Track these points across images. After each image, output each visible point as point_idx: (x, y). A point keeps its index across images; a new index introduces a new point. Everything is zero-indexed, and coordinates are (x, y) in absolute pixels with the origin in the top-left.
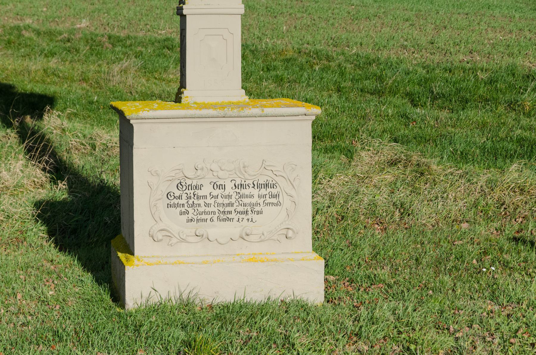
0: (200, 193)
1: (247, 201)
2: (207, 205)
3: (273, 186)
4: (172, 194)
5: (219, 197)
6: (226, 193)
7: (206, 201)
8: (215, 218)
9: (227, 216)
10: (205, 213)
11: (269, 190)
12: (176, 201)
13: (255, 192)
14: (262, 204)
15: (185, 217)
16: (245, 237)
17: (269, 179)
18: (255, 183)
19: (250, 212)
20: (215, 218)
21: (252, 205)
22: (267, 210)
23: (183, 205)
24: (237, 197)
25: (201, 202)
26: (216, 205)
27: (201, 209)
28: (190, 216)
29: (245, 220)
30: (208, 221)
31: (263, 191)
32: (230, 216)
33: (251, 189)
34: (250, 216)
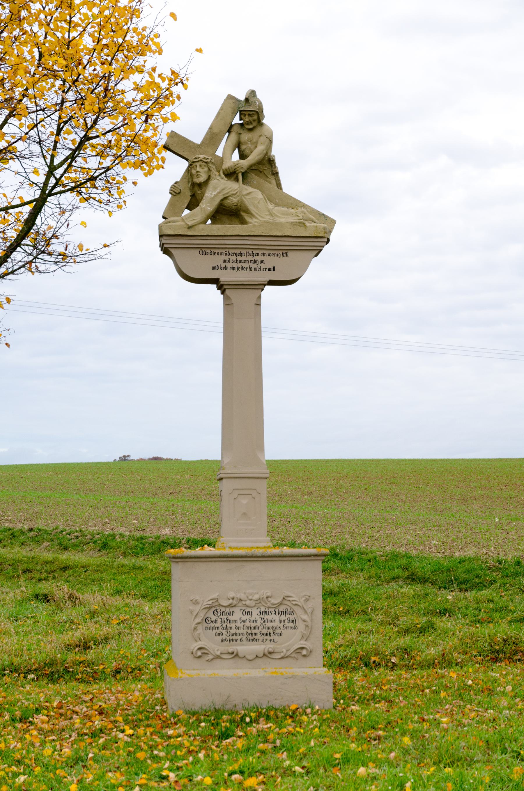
0: (232, 618)
1: (270, 625)
2: (238, 628)
3: (291, 613)
4: (209, 619)
5: (247, 621)
6: (253, 618)
7: (236, 624)
8: (244, 639)
9: (254, 637)
10: (236, 634)
11: (288, 616)
12: (212, 625)
13: (276, 617)
14: (282, 627)
15: (219, 638)
16: (269, 655)
17: (287, 607)
18: (277, 610)
19: (272, 634)
20: (244, 639)
21: (274, 628)
22: (285, 632)
23: (218, 628)
24: (262, 622)
25: (233, 625)
26: (245, 628)
27: (233, 631)
28: (224, 637)
29: (268, 641)
30: (239, 641)
31: (283, 617)
32: (256, 637)
33: (273, 615)
34: (272, 637)
